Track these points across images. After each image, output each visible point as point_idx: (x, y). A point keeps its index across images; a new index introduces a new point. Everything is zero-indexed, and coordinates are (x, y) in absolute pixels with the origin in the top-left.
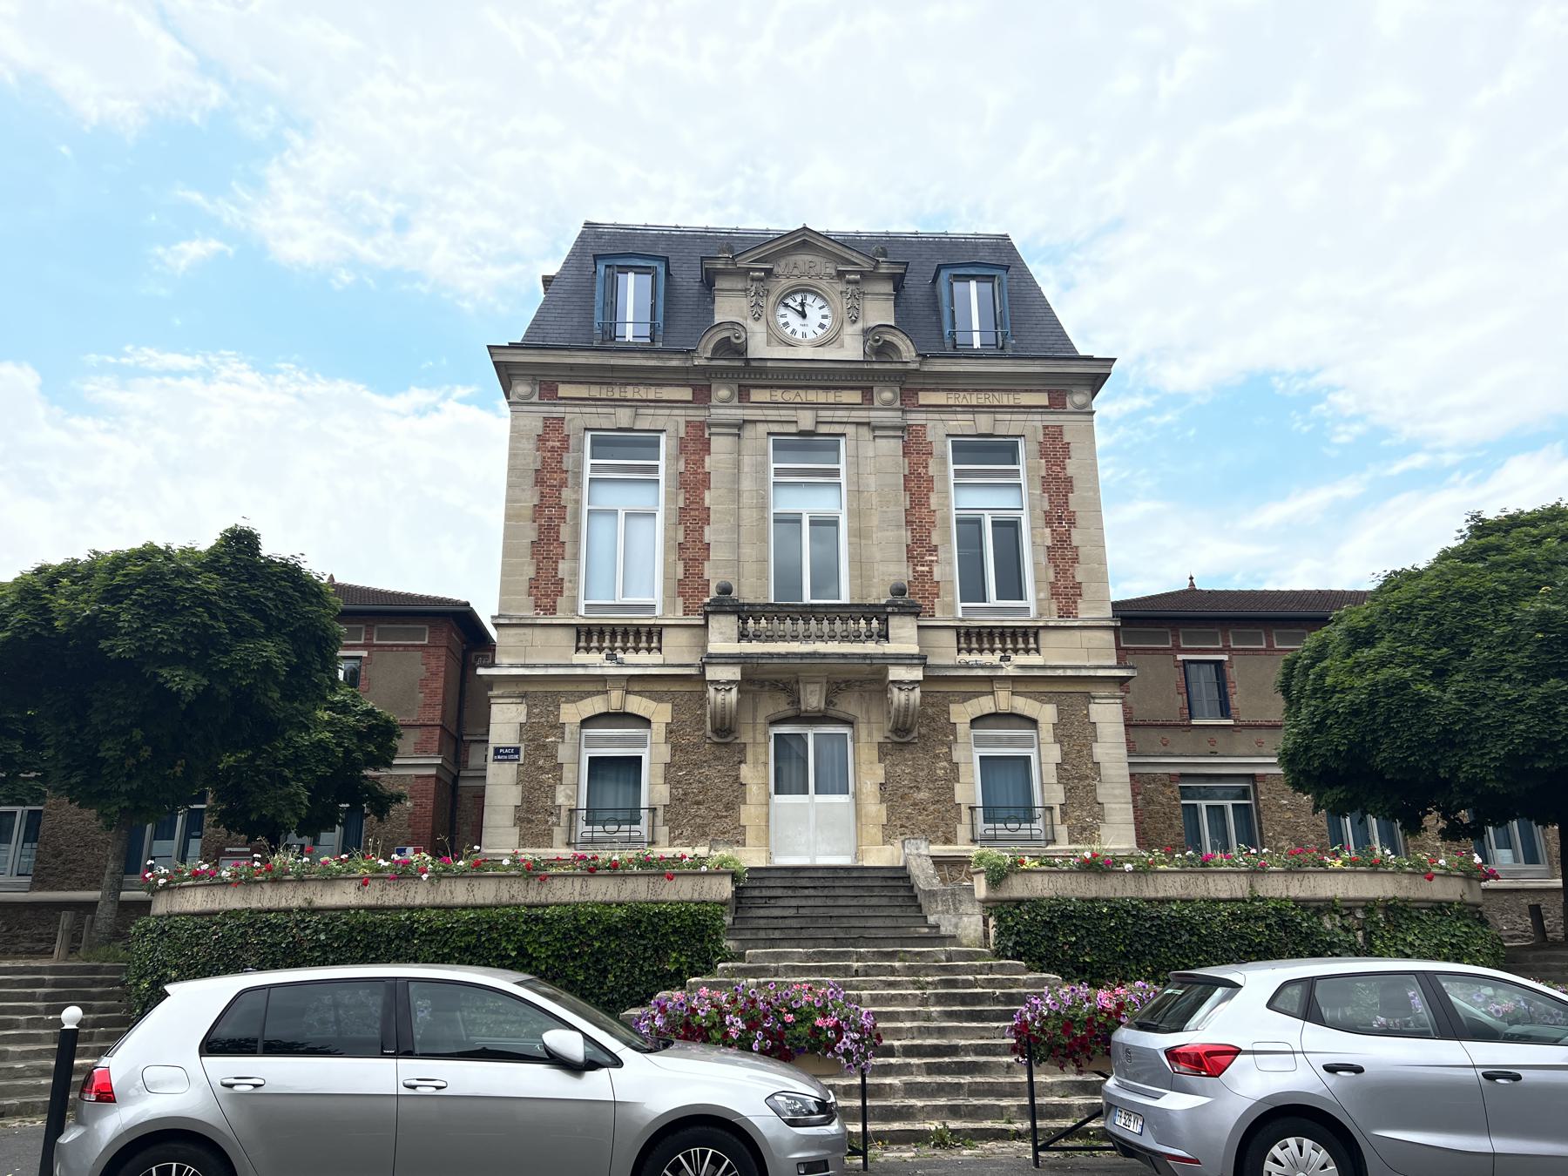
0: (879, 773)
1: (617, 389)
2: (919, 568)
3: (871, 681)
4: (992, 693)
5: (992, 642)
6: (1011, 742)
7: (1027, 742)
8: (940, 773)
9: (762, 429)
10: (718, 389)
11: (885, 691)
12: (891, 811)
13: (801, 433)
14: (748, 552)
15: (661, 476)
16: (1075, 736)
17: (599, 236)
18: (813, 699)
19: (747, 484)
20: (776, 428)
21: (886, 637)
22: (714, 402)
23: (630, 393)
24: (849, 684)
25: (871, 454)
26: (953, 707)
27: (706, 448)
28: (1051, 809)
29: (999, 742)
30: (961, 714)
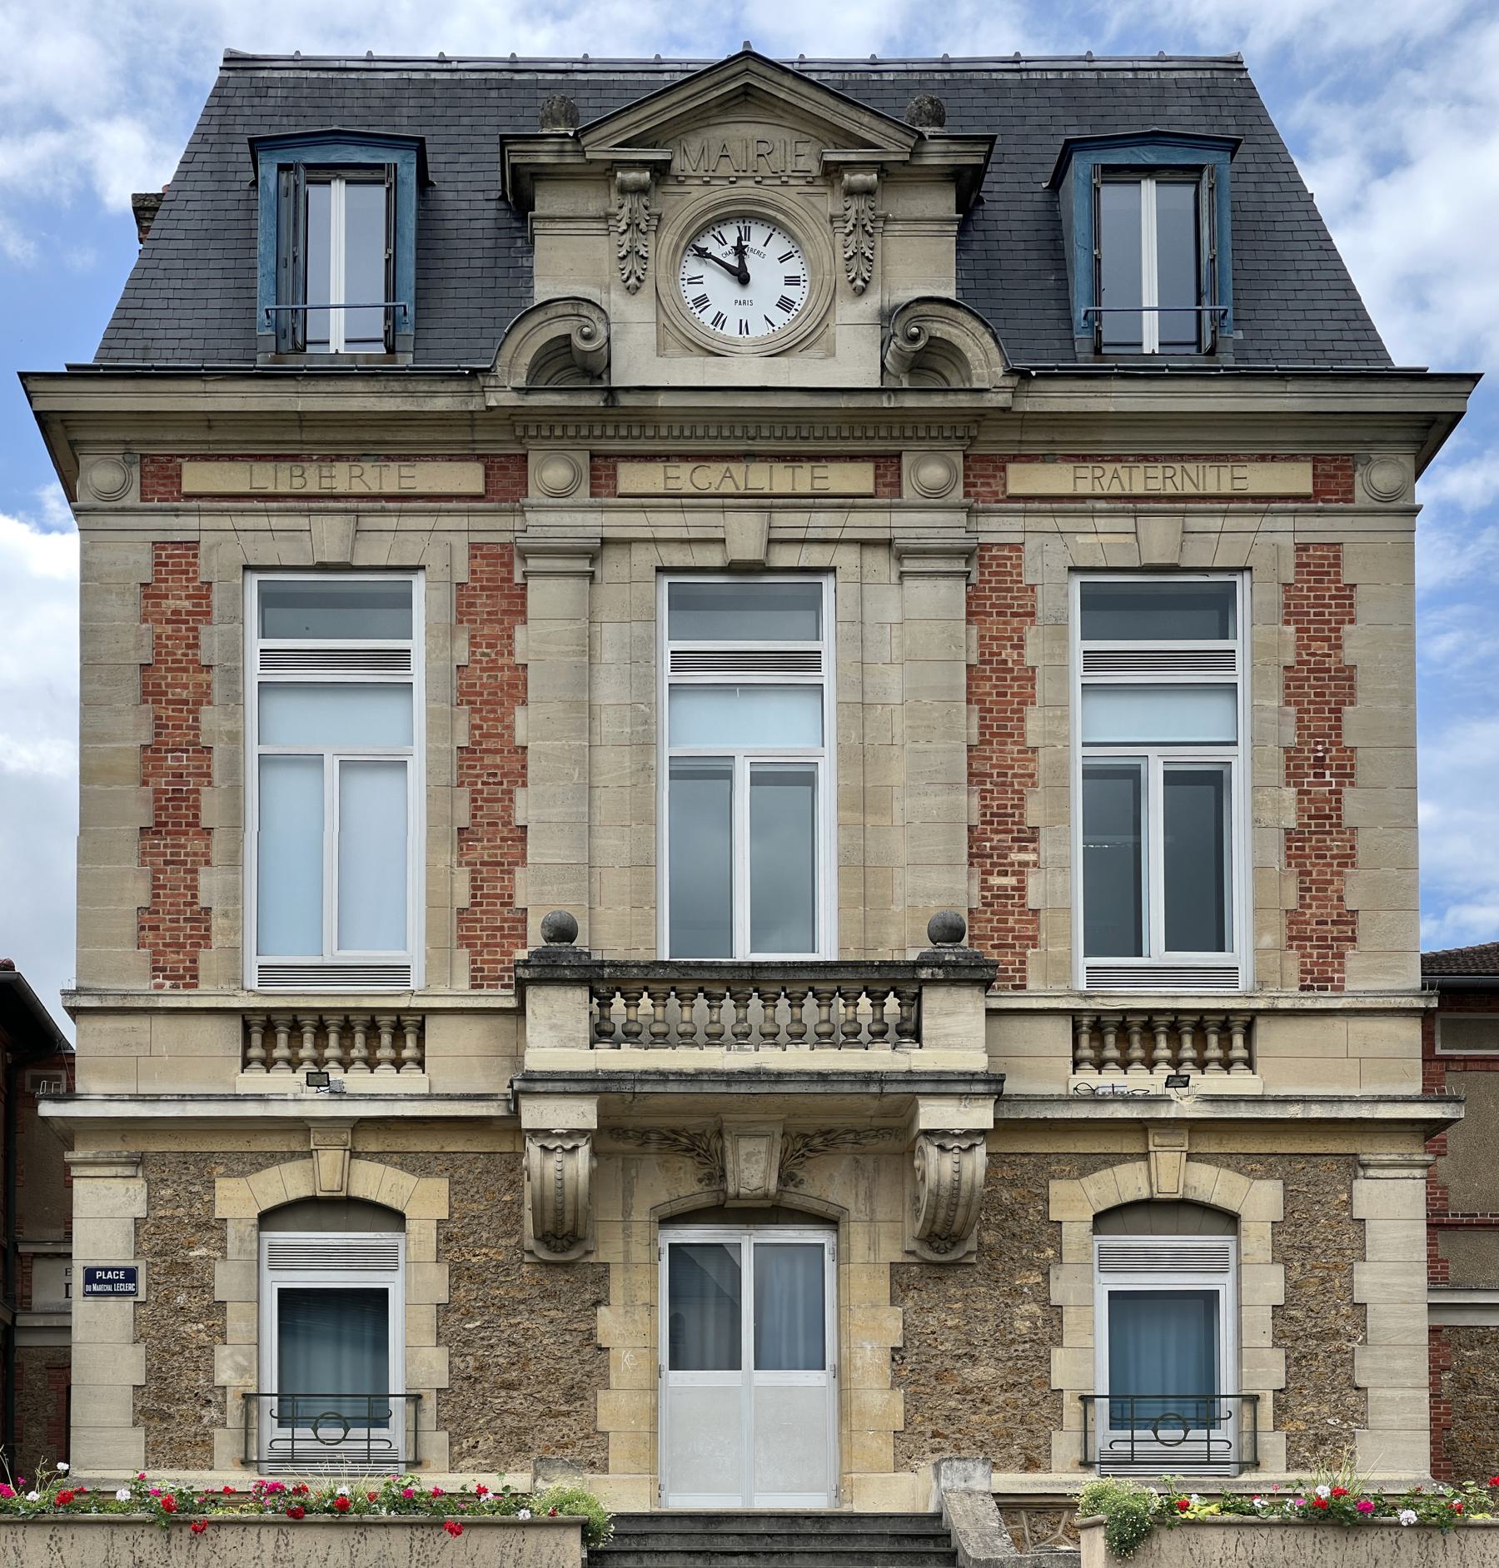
0: (890, 1325)
1: (312, 470)
2: (996, 880)
3: (880, 1132)
4: (1145, 1156)
5: (1150, 1043)
6: (1180, 1261)
7: (1214, 1262)
8: (1022, 1326)
9: (644, 558)
10: (541, 467)
11: (910, 1152)
12: (914, 1404)
13: (733, 568)
14: (612, 845)
15: (417, 673)
16: (1319, 1247)
17: (261, 91)
18: (752, 1170)
19: (610, 690)
20: (677, 557)
21: (912, 1032)
22: (535, 496)
23: (343, 478)
24: (830, 1138)
25: (894, 617)
26: (1057, 1188)
27: (517, 606)
28: (1254, 1400)
29: (1151, 1261)
30: (1074, 1201)
